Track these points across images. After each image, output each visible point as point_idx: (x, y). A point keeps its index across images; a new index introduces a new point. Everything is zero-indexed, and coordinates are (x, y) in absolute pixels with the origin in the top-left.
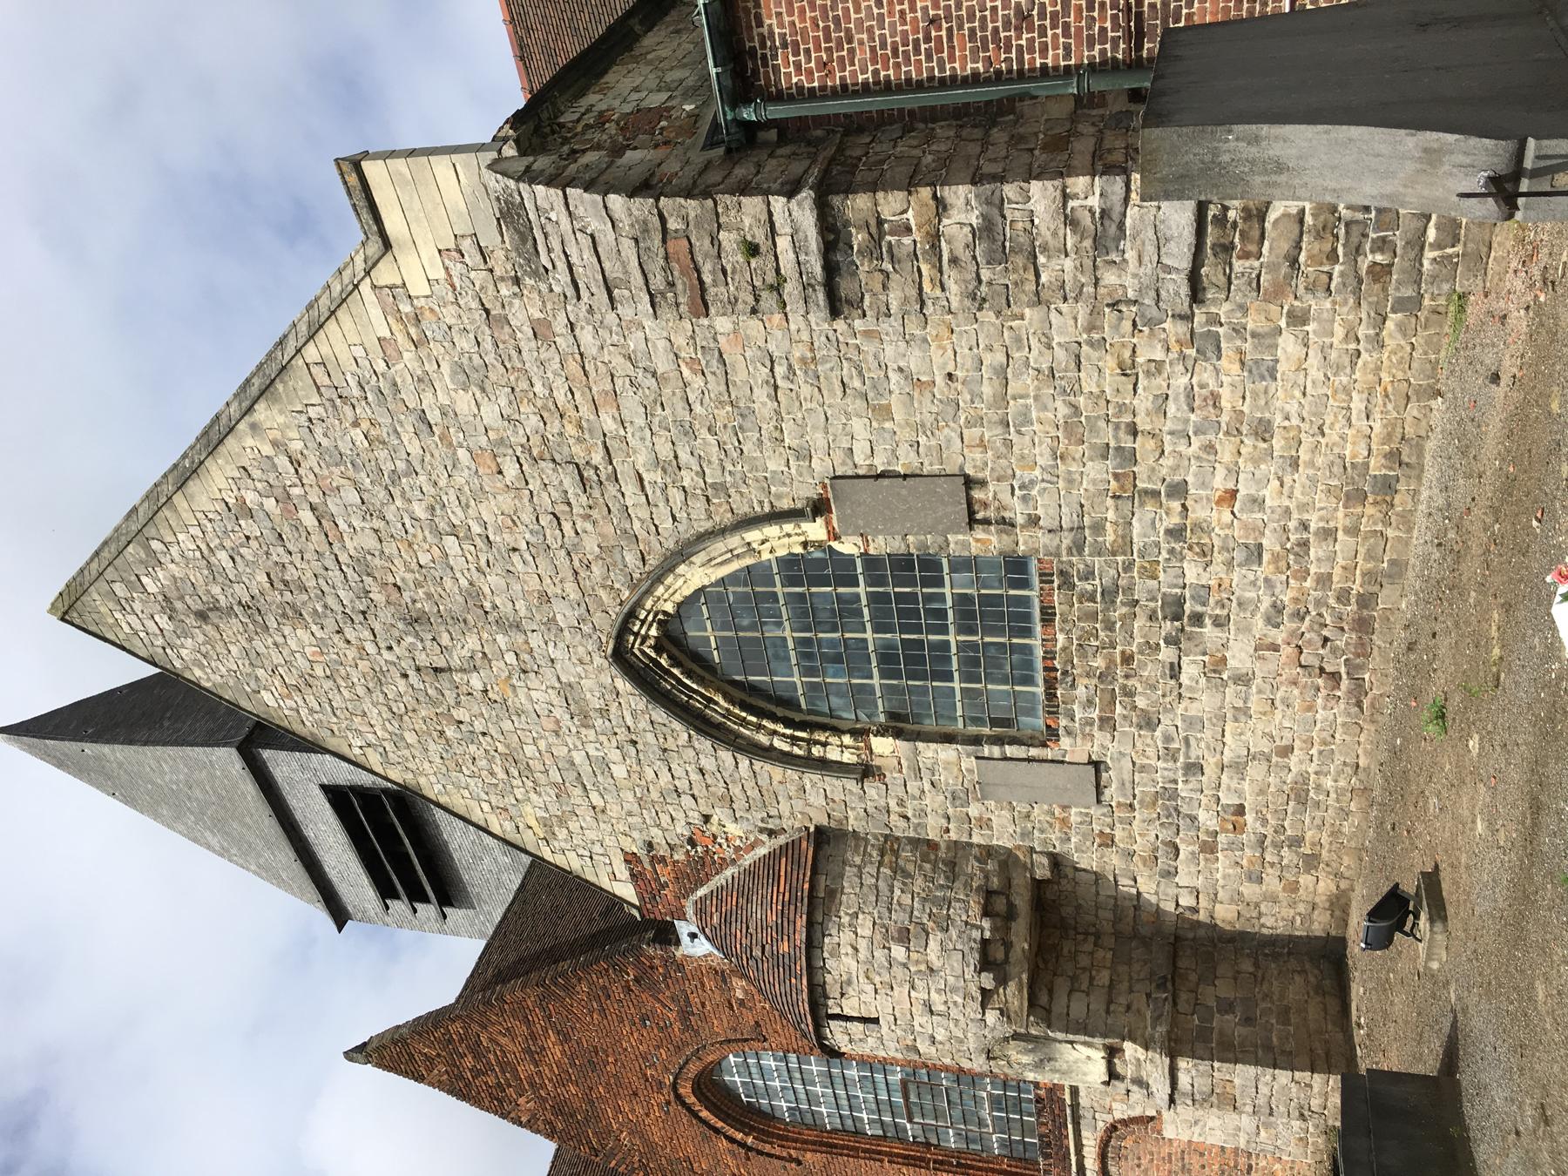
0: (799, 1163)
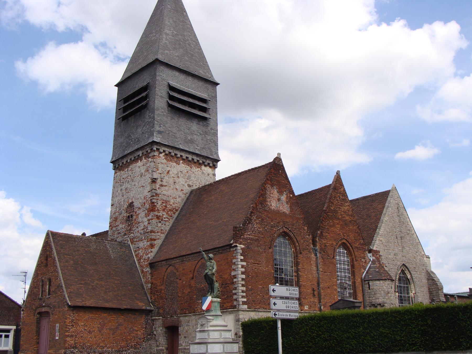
0: (333, 258)
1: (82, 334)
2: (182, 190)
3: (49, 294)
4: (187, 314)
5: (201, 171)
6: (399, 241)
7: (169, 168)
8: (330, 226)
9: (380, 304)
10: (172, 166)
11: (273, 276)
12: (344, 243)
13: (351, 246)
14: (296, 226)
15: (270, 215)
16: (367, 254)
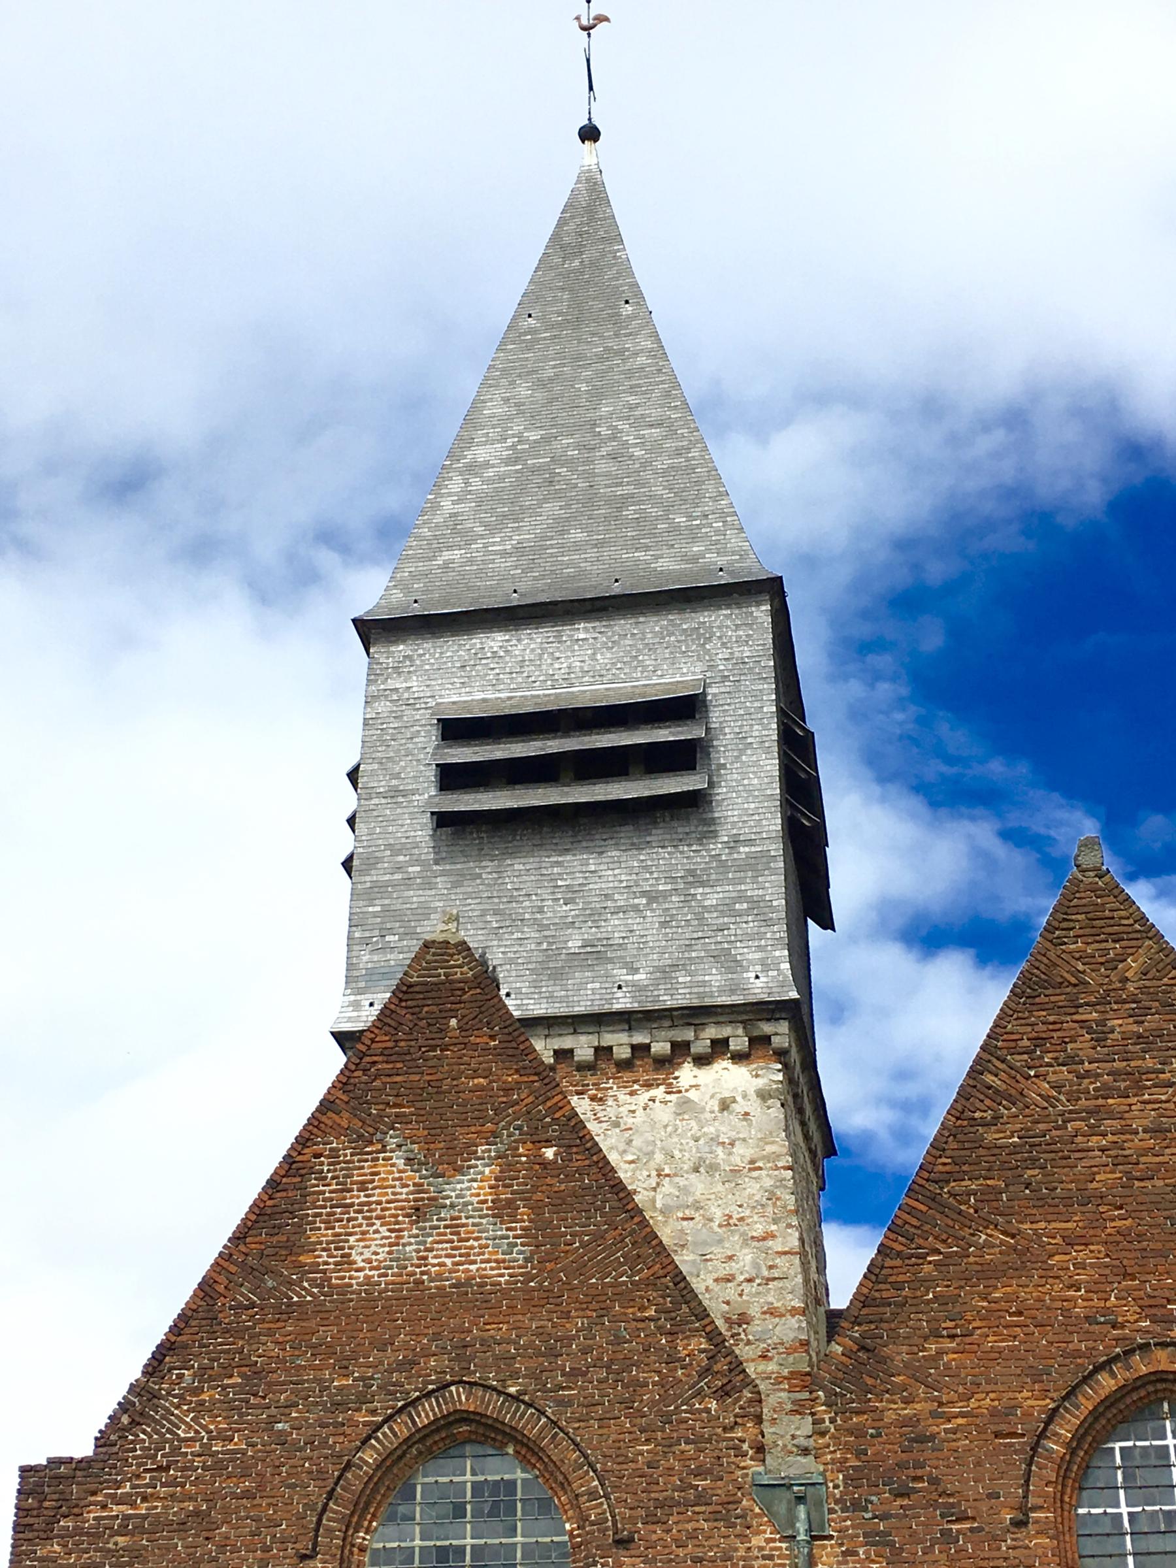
0: (1019, 1524)
5: (669, 1097)
8: (989, 1274)
14: (585, 1351)
15: (328, 1334)
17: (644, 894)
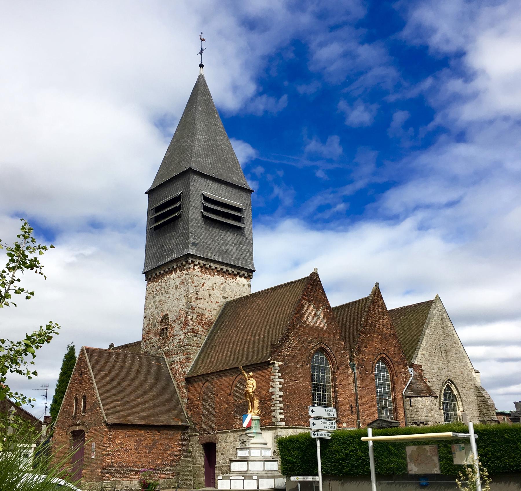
0: (372, 373)
1: (119, 452)
2: (217, 302)
3: (84, 412)
4: (225, 431)
5: (236, 282)
6: (444, 355)
7: (204, 280)
8: (369, 340)
9: (423, 423)
10: (207, 278)
11: (311, 392)
12: (383, 357)
13: (391, 361)
14: (333, 341)
15: (307, 331)
16: (408, 369)
17: (234, 243)
